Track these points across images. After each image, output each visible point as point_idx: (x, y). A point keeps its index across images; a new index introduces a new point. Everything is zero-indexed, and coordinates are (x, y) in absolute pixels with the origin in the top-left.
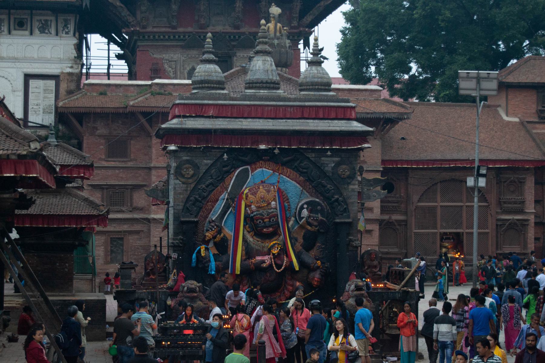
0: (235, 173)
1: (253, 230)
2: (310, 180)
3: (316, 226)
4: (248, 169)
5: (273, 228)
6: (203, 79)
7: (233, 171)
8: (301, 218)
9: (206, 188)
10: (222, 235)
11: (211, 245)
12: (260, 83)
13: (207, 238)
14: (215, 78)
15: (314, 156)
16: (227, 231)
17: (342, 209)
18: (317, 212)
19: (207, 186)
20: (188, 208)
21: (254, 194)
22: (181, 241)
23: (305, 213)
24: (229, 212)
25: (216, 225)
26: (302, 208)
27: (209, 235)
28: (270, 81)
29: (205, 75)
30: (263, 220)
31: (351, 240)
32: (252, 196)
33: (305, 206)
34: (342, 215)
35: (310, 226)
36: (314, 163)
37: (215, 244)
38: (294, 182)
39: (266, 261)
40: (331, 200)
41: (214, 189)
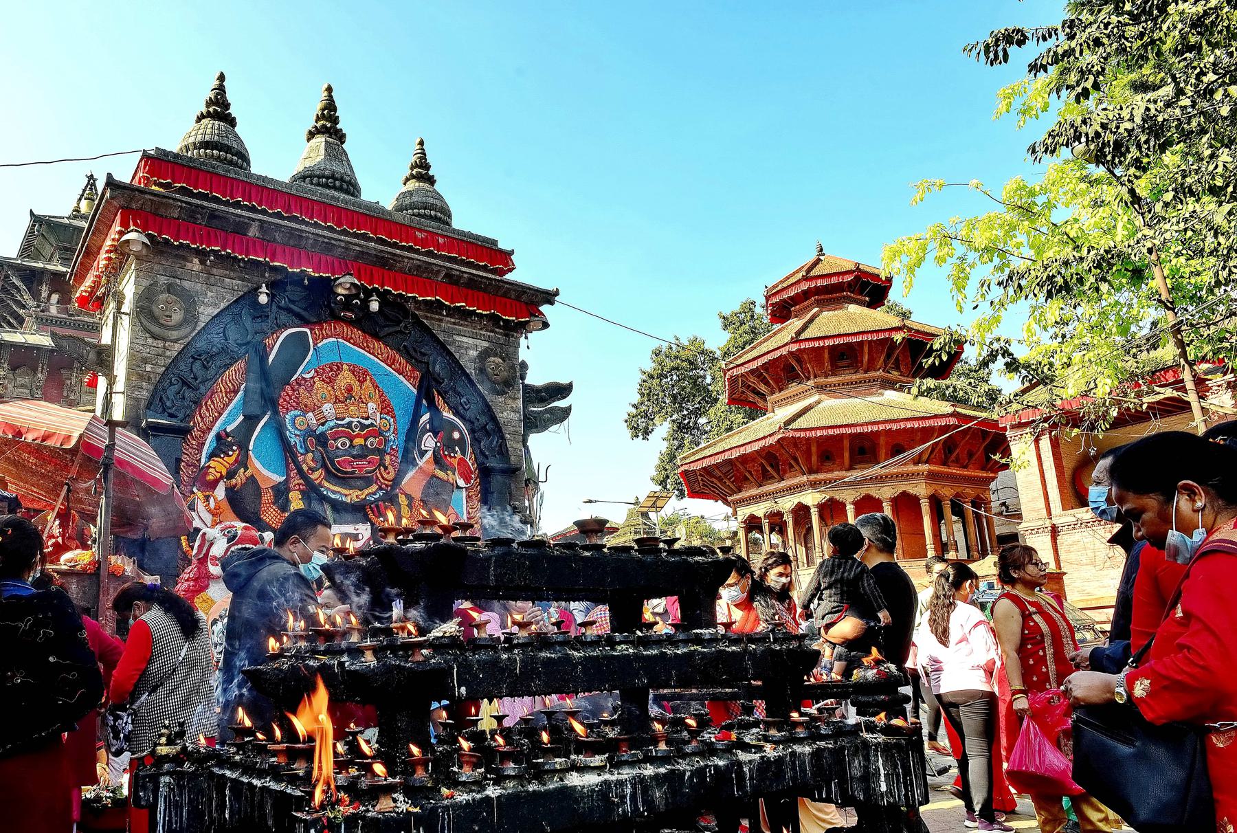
12: (328, 178)
27: (218, 467)
30: (351, 442)
36: (443, 348)
38: (401, 377)
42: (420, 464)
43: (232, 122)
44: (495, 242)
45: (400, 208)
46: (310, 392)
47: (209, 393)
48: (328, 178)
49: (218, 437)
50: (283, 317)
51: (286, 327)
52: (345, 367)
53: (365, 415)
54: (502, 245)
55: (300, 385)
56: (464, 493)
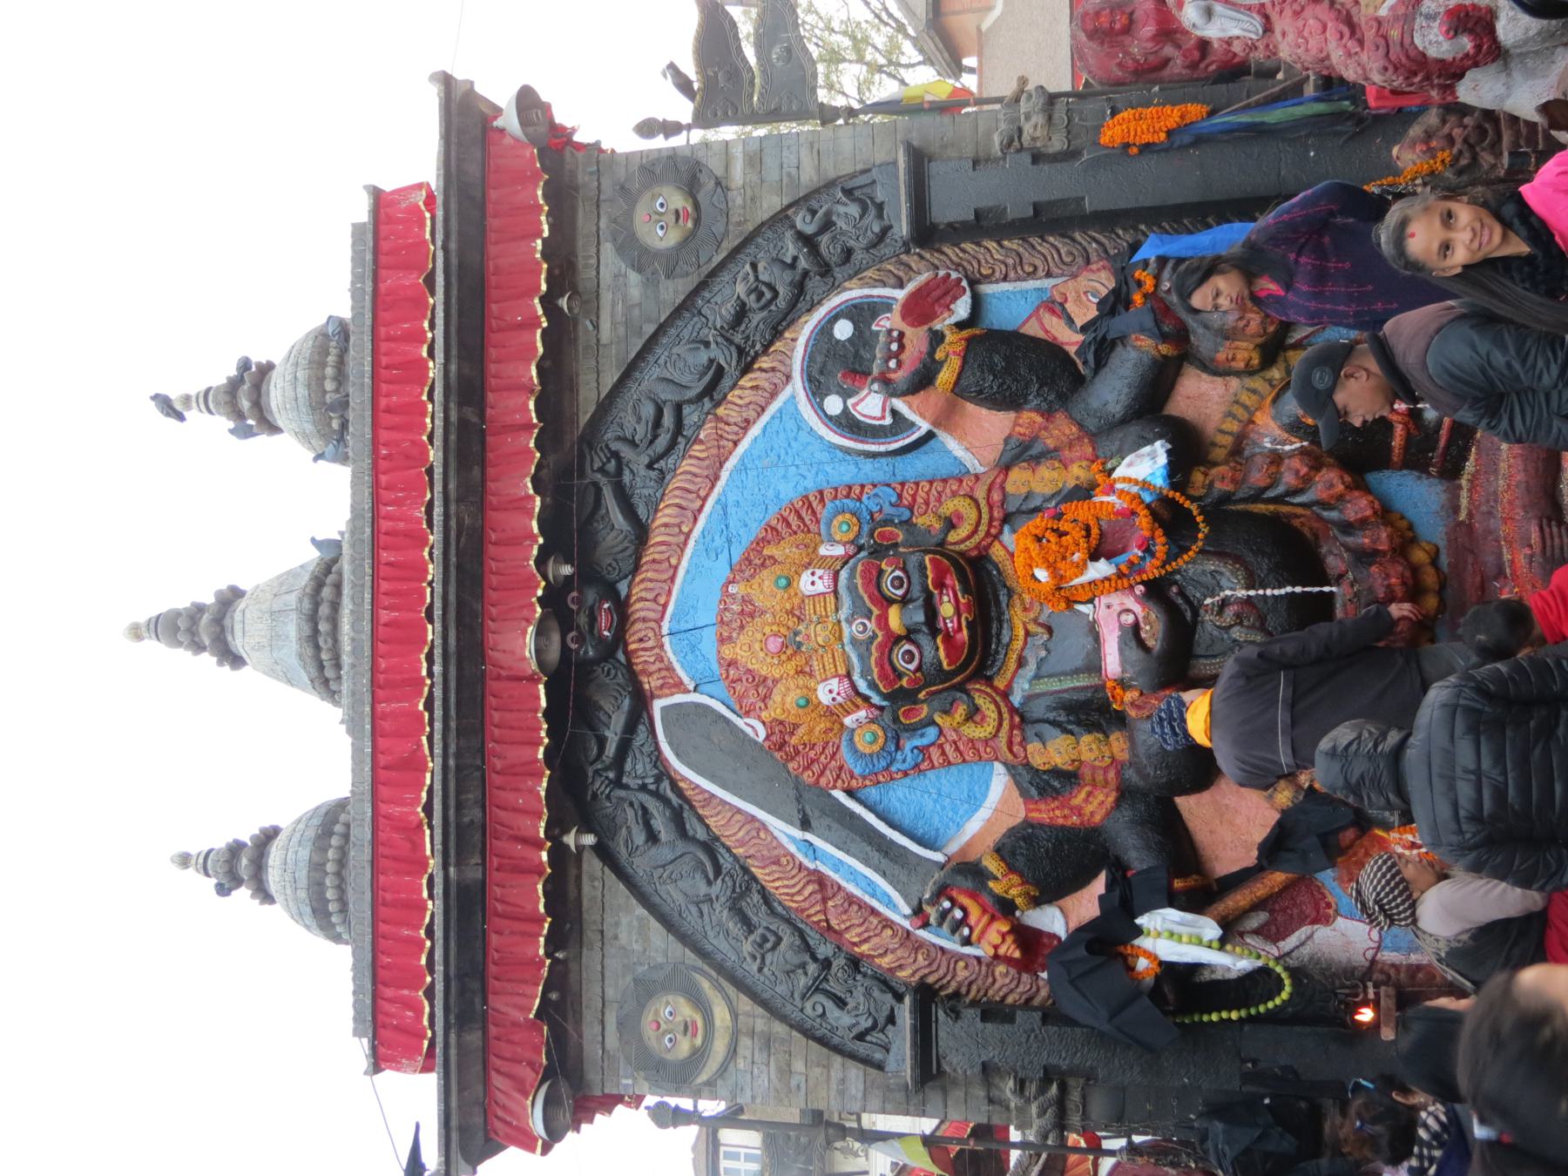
0: (684, 779)
1: (960, 688)
2: (713, 387)
3: (937, 338)
4: (664, 709)
5: (940, 585)
6: (308, 910)
9: (756, 936)
10: (992, 865)
12: (317, 648)
13: (1010, 949)
14: (305, 854)
16: (973, 826)
17: (854, 210)
18: (863, 337)
19: (749, 927)
20: (861, 1037)
21: (763, 686)
22: (1032, 1089)
23: (870, 405)
24: (870, 818)
25: (935, 900)
27: (994, 938)
28: (307, 605)
29: (296, 899)
30: (898, 640)
31: (1013, 140)
32: (777, 697)
33: (834, 404)
34: (880, 207)
35: (938, 371)
37: (1050, 891)
38: (724, 475)
39: (1130, 619)
40: (805, 274)
42: (924, 427)
43: (268, 836)
44: (358, 229)
45: (343, 459)
46: (796, 726)
47: (831, 937)
48: (317, 648)
51: (657, 758)
52: (728, 652)
53: (831, 599)
54: (362, 214)
56: (987, 289)
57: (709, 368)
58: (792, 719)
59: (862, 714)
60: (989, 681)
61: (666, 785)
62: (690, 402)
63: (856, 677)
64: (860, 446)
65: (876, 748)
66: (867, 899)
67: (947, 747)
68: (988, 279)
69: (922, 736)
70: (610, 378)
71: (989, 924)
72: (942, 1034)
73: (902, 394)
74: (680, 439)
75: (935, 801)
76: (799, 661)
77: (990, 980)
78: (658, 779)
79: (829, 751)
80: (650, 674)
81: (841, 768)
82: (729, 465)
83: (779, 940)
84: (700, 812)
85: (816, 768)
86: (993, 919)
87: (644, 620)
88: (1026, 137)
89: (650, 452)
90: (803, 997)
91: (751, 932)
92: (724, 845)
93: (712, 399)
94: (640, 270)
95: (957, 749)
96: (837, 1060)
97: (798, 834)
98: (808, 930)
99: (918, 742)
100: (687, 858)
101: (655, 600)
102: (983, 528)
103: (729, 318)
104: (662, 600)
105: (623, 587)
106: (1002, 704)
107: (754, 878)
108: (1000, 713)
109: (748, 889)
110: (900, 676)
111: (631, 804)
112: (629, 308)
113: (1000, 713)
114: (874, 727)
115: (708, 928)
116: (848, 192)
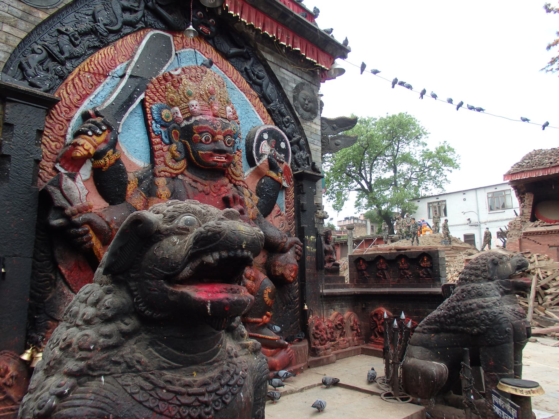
2: (265, 99)
7: (142, 28)
8: (260, 156)
11: (86, 172)
13: (80, 152)
15: (273, 61)
18: (281, 150)
20: (21, 67)
23: (265, 148)
25: (105, 123)
26: (261, 139)
27: (87, 145)
30: (213, 136)
32: (191, 83)
33: (266, 136)
38: (243, 93)
41: (97, 48)
42: (258, 164)
49: (86, 116)
50: (150, 19)
55: (167, 81)
57: (271, 99)
58: (181, 87)
59: (180, 115)
60: (187, 168)
61: (144, 26)
62: (262, 90)
63: (201, 117)
64: (255, 141)
65: (163, 117)
66: (96, 93)
67: (160, 145)
68: (287, 194)
69: (166, 137)
70: (273, 67)
71: (92, 144)
72: (29, 107)
73: (269, 160)
74: (251, 82)
75: (135, 135)
76: (205, 97)
77: (54, 139)
78: (145, 23)
79: (161, 98)
80: (182, 38)
81: (154, 100)
82: (244, 95)
83: (75, 46)
84: (133, 35)
85: (154, 90)
86: (95, 147)
87: (200, 45)
88: (318, 211)
89: (250, 71)
90: (44, 46)
91: (79, 34)
92: (119, 39)
93: (262, 97)
94: (296, 88)
95: (160, 149)
96: (10, 51)
97: (129, 72)
98: (79, 61)
99: (163, 134)
100: (114, 20)
101: (206, 52)
102: (234, 177)
103: (282, 111)
104: (206, 54)
105: (210, 42)
106: (180, 171)
107: (106, 45)
108: (176, 170)
109: (101, 42)
110: (200, 133)
111: (138, 7)
112: (287, 80)
113: (176, 170)
114: (171, 119)
115: (80, 15)
116: (308, 158)
